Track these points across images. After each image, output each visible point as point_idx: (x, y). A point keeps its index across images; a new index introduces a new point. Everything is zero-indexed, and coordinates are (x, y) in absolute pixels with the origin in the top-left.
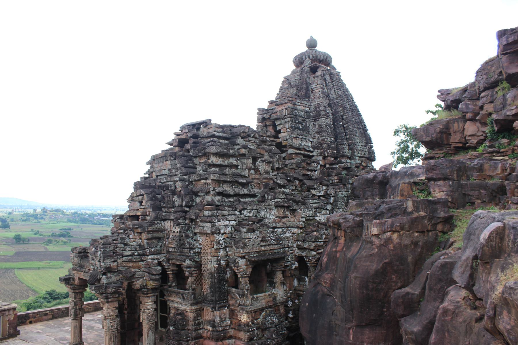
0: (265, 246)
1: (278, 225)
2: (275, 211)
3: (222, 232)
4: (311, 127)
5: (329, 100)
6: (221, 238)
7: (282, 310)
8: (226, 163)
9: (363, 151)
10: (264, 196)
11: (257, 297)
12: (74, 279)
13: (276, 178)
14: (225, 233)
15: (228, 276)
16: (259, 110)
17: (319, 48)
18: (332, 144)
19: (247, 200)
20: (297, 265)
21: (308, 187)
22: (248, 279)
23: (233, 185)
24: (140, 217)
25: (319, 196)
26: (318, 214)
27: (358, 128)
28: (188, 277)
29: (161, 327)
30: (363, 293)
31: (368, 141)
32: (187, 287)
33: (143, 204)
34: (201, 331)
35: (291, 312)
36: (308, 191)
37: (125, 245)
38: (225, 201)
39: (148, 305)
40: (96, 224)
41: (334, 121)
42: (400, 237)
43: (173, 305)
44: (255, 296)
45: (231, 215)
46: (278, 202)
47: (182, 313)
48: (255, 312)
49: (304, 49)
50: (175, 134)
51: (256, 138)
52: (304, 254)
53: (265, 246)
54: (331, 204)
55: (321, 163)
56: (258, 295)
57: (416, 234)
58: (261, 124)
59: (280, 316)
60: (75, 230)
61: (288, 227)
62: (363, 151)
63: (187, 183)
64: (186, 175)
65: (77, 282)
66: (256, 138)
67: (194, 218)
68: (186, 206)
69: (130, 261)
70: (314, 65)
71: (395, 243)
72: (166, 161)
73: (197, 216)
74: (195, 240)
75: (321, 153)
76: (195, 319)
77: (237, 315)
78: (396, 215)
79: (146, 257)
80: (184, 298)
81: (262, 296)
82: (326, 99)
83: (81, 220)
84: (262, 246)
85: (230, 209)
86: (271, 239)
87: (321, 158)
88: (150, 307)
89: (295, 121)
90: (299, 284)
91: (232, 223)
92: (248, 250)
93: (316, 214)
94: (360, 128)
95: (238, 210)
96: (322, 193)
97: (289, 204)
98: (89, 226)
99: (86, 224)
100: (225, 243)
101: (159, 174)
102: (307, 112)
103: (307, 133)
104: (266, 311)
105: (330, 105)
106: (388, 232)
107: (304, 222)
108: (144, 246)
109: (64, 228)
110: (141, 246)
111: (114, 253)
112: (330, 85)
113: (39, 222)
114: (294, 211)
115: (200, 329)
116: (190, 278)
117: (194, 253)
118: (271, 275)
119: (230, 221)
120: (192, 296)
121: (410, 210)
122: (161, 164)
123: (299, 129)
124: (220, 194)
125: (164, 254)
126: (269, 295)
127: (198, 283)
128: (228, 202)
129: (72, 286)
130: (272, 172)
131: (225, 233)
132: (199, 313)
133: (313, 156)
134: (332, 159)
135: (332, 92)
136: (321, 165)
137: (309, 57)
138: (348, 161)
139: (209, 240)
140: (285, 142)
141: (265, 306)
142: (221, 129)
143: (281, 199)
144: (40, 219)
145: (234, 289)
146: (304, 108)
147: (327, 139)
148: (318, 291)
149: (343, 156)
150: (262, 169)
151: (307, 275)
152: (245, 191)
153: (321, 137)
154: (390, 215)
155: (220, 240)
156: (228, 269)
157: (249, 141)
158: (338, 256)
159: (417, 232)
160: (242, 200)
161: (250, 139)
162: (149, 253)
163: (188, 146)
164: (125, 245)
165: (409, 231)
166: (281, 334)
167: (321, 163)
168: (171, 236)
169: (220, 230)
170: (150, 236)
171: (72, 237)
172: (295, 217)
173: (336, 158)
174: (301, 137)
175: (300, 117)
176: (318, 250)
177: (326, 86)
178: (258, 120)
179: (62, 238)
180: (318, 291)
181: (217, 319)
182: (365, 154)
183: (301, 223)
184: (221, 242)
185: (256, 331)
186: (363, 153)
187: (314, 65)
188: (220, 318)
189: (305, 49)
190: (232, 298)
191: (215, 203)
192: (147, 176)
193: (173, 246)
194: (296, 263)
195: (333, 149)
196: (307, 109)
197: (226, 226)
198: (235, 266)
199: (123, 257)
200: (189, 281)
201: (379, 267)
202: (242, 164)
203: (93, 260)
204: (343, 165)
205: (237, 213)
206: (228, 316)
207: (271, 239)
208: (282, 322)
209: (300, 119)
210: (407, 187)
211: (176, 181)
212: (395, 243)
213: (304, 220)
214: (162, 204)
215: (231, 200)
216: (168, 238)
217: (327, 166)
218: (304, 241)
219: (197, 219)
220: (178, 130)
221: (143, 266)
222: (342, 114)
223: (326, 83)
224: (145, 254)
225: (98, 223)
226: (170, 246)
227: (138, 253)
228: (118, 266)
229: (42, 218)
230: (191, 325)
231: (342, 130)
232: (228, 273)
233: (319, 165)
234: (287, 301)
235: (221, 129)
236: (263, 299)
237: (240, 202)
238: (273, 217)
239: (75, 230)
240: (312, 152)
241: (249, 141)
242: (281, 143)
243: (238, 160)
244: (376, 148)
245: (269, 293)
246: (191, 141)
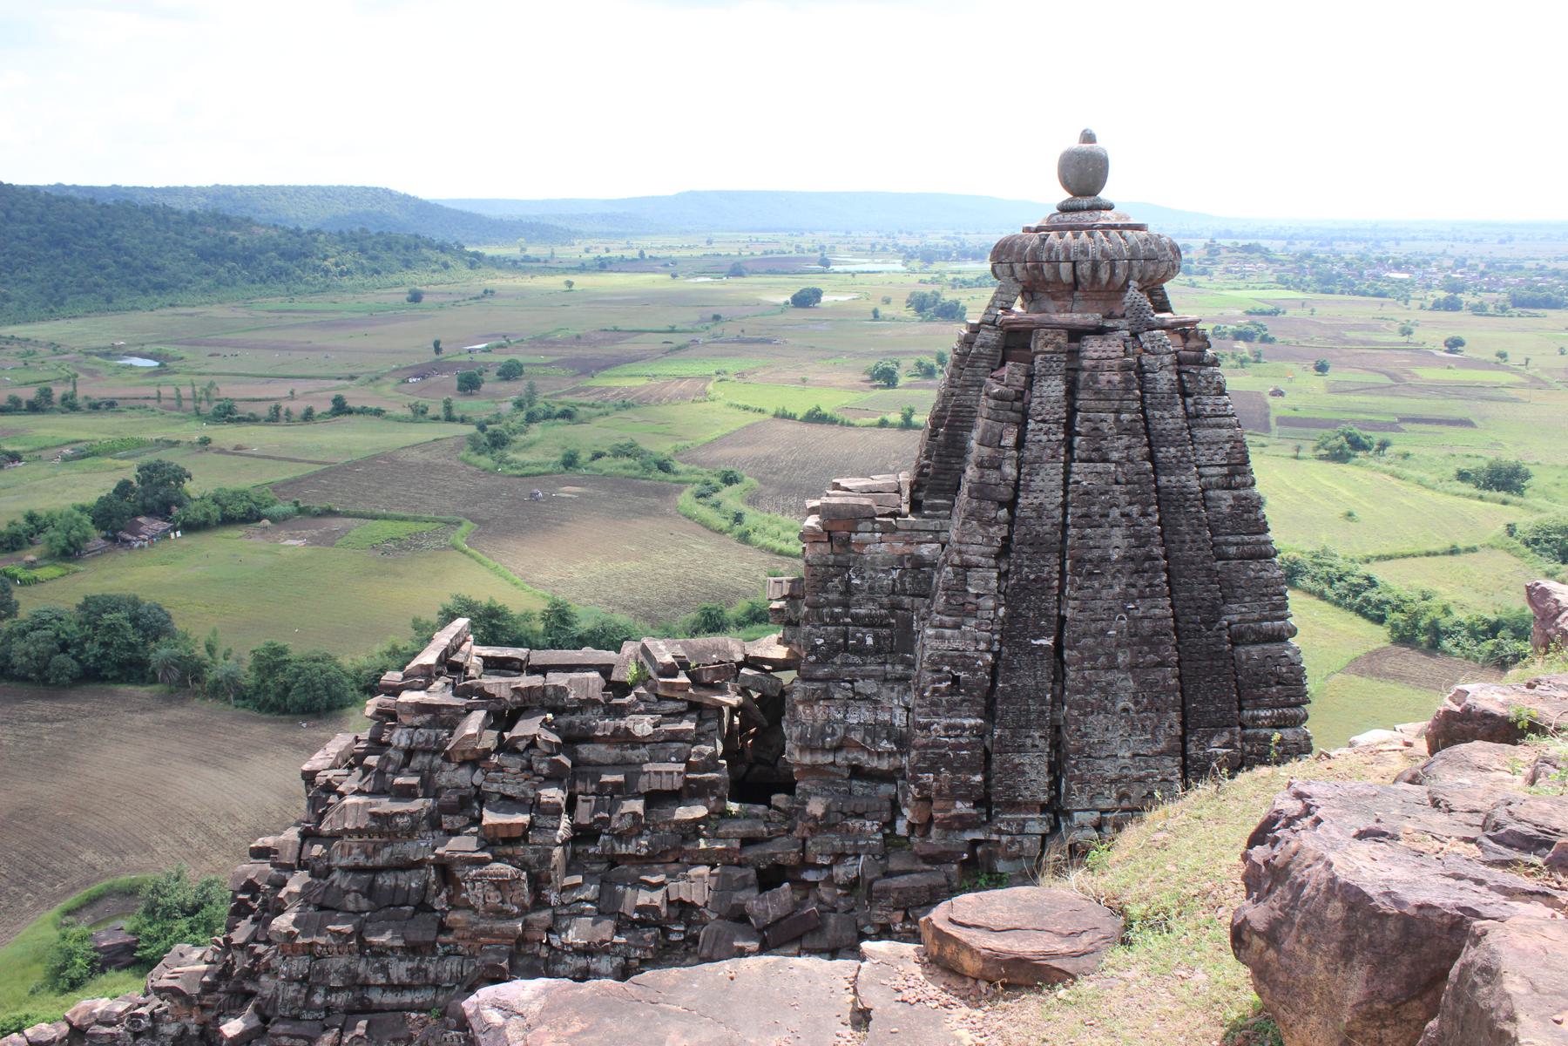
5: (1011, 523)
8: (382, 858)
17: (1123, 193)
19: (408, 998)
37: (137, 1035)
40: (1364, 294)
41: (1012, 631)
60: (1290, 313)
83: (1319, 281)
98: (1339, 302)
99: (1332, 292)
102: (919, 563)
103: (903, 661)
109: (1259, 306)
112: (1044, 435)
113: (1194, 285)
123: (860, 650)
128: (318, 1009)
144: (1197, 274)
149: (1013, 805)
152: (400, 970)
164: (137, 1035)
171: (1272, 340)
173: (983, 801)
179: (1241, 345)
196: (925, 550)
225: (1371, 291)
229: (1204, 272)
235: (428, 717)
239: (1290, 313)
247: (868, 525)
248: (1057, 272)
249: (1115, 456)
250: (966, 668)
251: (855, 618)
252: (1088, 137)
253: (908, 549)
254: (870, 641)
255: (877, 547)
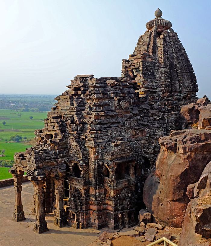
0: (124, 154)
1: (132, 140)
2: (130, 132)
3: (100, 146)
4: (155, 73)
5: (168, 54)
6: (100, 149)
7: (134, 188)
9: (189, 87)
10: (124, 123)
11: (120, 182)
12: (17, 171)
13: (132, 110)
14: (102, 146)
15: (104, 170)
16: (123, 60)
18: (169, 84)
20: (144, 162)
21: (151, 114)
22: (114, 172)
23: (106, 117)
24: (54, 136)
25: (159, 120)
26: (157, 131)
27: (186, 72)
28: (81, 171)
29: (65, 196)
30: (175, 184)
31: (193, 78)
32: (81, 176)
33: (55, 127)
34: (89, 200)
35: (139, 189)
36: (152, 116)
37: (46, 153)
38: (102, 128)
39: (59, 186)
42: (196, 155)
43: (73, 185)
44: (118, 181)
45: (105, 136)
46: (132, 126)
47: (77, 190)
48: (118, 190)
49: (153, 17)
50: (71, 81)
51: (121, 86)
52: (147, 156)
53: (124, 154)
54: (165, 123)
55: (161, 96)
56: (120, 181)
57: (205, 153)
58: (124, 70)
59: (132, 193)
61: (138, 141)
62: (189, 87)
63: (80, 116)
64: (79, 112)
65: (18, 173)
66: (121, 86)
67: (85, 138)
68: (80, 131)
69: (49, 162)
70: (160, 29)
71: (193, 158)
72: (68, 101)
73: (86, 137)
74: (85, 150)
75: (161, 90)
76: (85, 194)
77: (108, 191)
78: (194, 142)
79: (58, 159)
80: (79, 182)
81: (123, 181)
82: (166, 55)
84: (122, 154)
85: (105, 132)
86: (127, 149)
87: (161, 93)
88: (60, 187)
89: (145, 69)
90: (145, 173)
91: (106, 140)
92: (115, 156)
93: (156, 131)
94: (188, 72)
95: (109, 133)
96: (160, 118)
97: (139, 128)
100: (102, 152)
101: (63, 108)
102: (153, 62)
103: (153, 77)
104: (125, 190)
105: (168, 59)
106: (189, 152)
107: (148, 137)
108: (56, 153)
110: (55, 153)
111: (41, 158)
114: (142, 131)
115: (88, 199)
116: (82, 171)
117: (85, 157)
118: (128, 169)
119: (104, 139)
120: (84, 181)
121: (203, 139)
122: (64, 103)
123: (148, 75)
124: (99, 123)
125: (68, 157)
126: (126, 180)
127: (87, 173)
129: (16, 175)
130: (130, 106)
131: (102, 146)
132: (87, 191)
133: (157, 91)
134: (169, 93)
135: (170, 49)
136: (161, 98)
137: (156, 24)
138: (179, 94)
139: (93, 151)
140: (139, 83)
141: (124, 187)
142: (100, 82)
143: (134, 124)
145: (107, 178)
146: (152, 60)
147: (165, 81)
148: (153, 179)
149: (176, 92)
150: (123, 106)
151: (149, 168)
152: (114, 120)
153: (162, 80)
154: (190, 142)
155: (99, 151)
156: (103, 166)
157: (116, 88)
158: (164, 161)
159: (206, 151)
160: (112, 126)
161: (117, 87)
162: (60, 157)
163: (79, 92)
164: (46, 153)
165: (201, 151)
166: (133, 202)
167: (161, 96)
168: (71, 147)
169: (99, 145)
170: (60, 147)
172: (142, 134)
173: (171, 93)
174: (149, 80)
175: (149, 66)
176: (156, 153)
177: (166, 45)
178: (123, 67)
180: (153, 179)
181: (98, 194)
182: (190, 89)
183: (146, 138)
184: (99, 152)
185: (118, 201)
186: (189, 89)
187: (160, 29)
188: (99, 193)
189: (153, 17)
190: (106, 182)
191: (96, 129)
192: (55, 107)
193: (72, 153)
194: (143, 161)
195: (169, 87)
196: (154, 61)
197: (102, 143)
198: (107, 165)
199: (46, 160)
200: (82, 172)
201: (183, 171)
202: (112, 103)
203: (29, 161)
204: (175, 97)
205: (109, 134)
206: (103, 192)
207: (127, 149)
208: (133, 195)
209: (149, 68)
210: (206, 122)
211: (74, 115)
212: (193, 158)
213: (148, 135)
214: (66, 128)
215: (105, 126)
216: (70, 148)
217: (165, 98)
218: (147, 148)
219: (86, 138)
220: (73, 79)
221: (56, 164)
222: (176, 63)
223: (166, 43)
224: (57, 158)
226: (71, 153)
227: (54, 157)
228: (43, 165)
230: (83, 198)
231: (175, 74)
232: (104, 169)
233: (160, 98)
234: (137, 184)
235: (100, 82)
236: (123, 183)
237: (110, 127)
238: (129, 135)
240: (156, 89)
241: (116, 88)
242: (136, 83)
243: (109, 100)
244: (198, 83)
245: (126, 179)
246: (82, 89)
247: (148, 56)
248: (163, 25)
249: (177, 47)
250: (167, 73)
251: (148, 69)
252: (159, 9)
253: (152, 60)
254: (149, 73)
255: (149, 60)
